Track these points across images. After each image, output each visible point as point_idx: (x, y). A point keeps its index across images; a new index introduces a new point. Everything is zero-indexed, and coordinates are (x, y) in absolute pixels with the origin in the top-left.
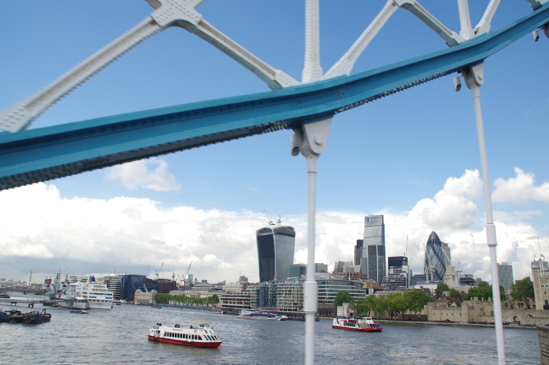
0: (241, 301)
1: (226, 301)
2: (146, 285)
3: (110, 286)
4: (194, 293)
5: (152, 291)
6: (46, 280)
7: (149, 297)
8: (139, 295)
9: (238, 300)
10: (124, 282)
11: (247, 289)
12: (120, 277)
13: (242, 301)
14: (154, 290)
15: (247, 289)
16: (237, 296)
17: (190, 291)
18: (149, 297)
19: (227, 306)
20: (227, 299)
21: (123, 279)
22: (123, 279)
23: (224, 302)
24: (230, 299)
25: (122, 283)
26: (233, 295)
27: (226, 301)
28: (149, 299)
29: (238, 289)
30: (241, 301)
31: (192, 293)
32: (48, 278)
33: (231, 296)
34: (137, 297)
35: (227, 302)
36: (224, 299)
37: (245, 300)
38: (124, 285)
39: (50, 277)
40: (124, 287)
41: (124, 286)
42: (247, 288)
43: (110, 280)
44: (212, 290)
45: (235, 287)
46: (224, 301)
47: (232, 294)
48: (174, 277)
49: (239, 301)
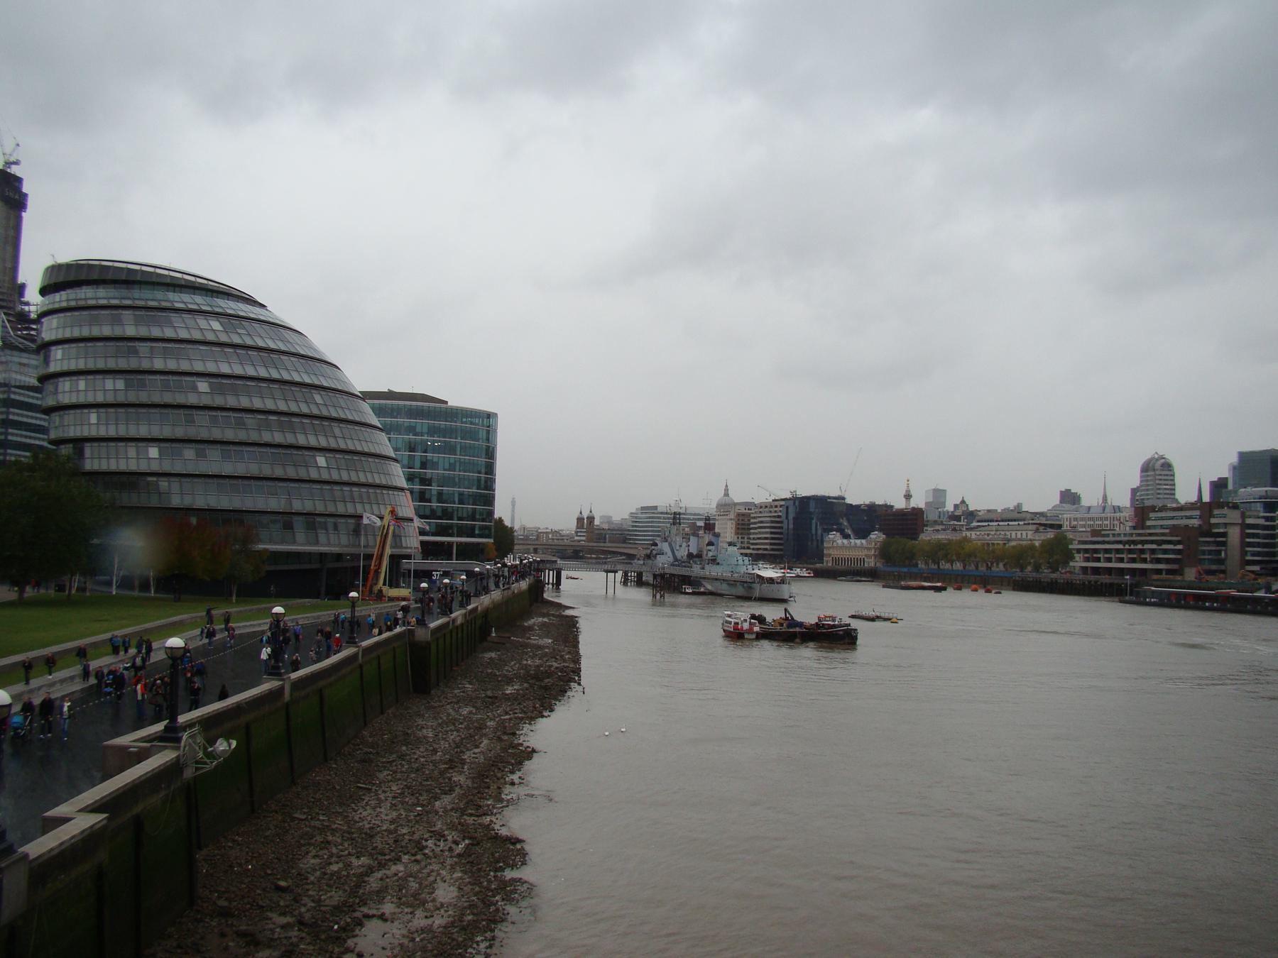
0: (1143, 556)
1: (1095, 555)
2: (848, 520)
3: (752, 526)
4: (991, 536)
5: (873, 536)
6: (580, 520)
7: (866, 552)
8: (838, 545)
9: (1130, 551)
10: (791, 516)
11: (1149, 523)
12: (776, 503)
13: (1147, 556)
14: (876, 532)
15: (1149, 523)
16: (1129, 542)
17: (978, 533)
18: (866, 552)
19: (1096, 571)
20: (1096, 551)
21: (787, 508)
22: (787, 508)
23: (1087, 560)
24: (1107, 551)
25: (787, 518)
26: (1111, 538)
27: (1095, 555)
28: (866, 555)
29: (1108, 522)
30: (1143, 556)
31: (986, 536)
32: (585, 515)
33: (1104, 542)
34: (831, 552)
35: (1098, 560)
36: (1086, 551)
37: (1153, 551)
38: (791, 522)
39: (591, 512)
40: (794, 529)
41: (791, 526)
42: (1149, 519)
43: (747, 511)
44: (1041, 528)
45: (1101, 519)
46: (1086, 555)
47: (1108, 535)
48: (908, 496)
49: (1135, 556)
